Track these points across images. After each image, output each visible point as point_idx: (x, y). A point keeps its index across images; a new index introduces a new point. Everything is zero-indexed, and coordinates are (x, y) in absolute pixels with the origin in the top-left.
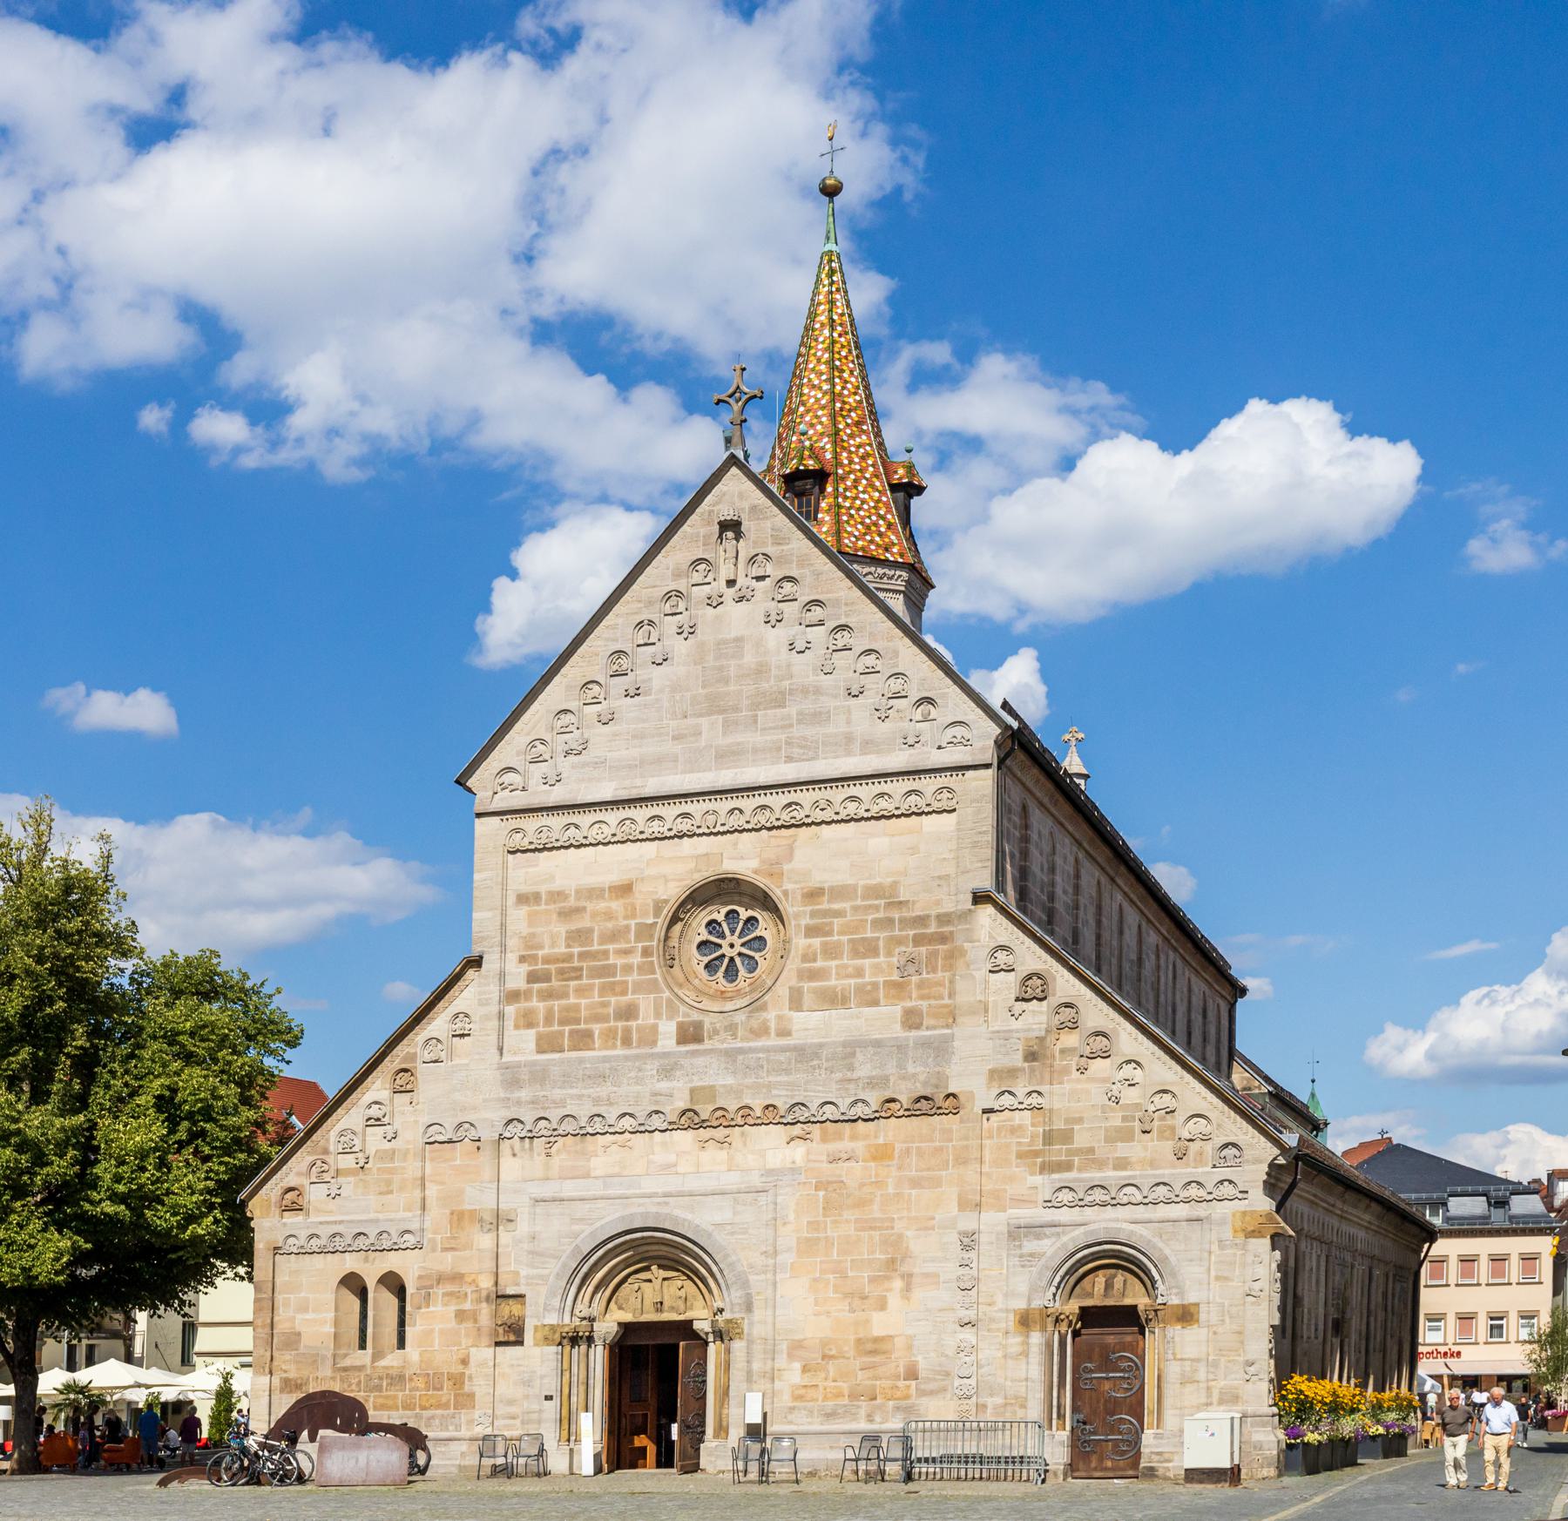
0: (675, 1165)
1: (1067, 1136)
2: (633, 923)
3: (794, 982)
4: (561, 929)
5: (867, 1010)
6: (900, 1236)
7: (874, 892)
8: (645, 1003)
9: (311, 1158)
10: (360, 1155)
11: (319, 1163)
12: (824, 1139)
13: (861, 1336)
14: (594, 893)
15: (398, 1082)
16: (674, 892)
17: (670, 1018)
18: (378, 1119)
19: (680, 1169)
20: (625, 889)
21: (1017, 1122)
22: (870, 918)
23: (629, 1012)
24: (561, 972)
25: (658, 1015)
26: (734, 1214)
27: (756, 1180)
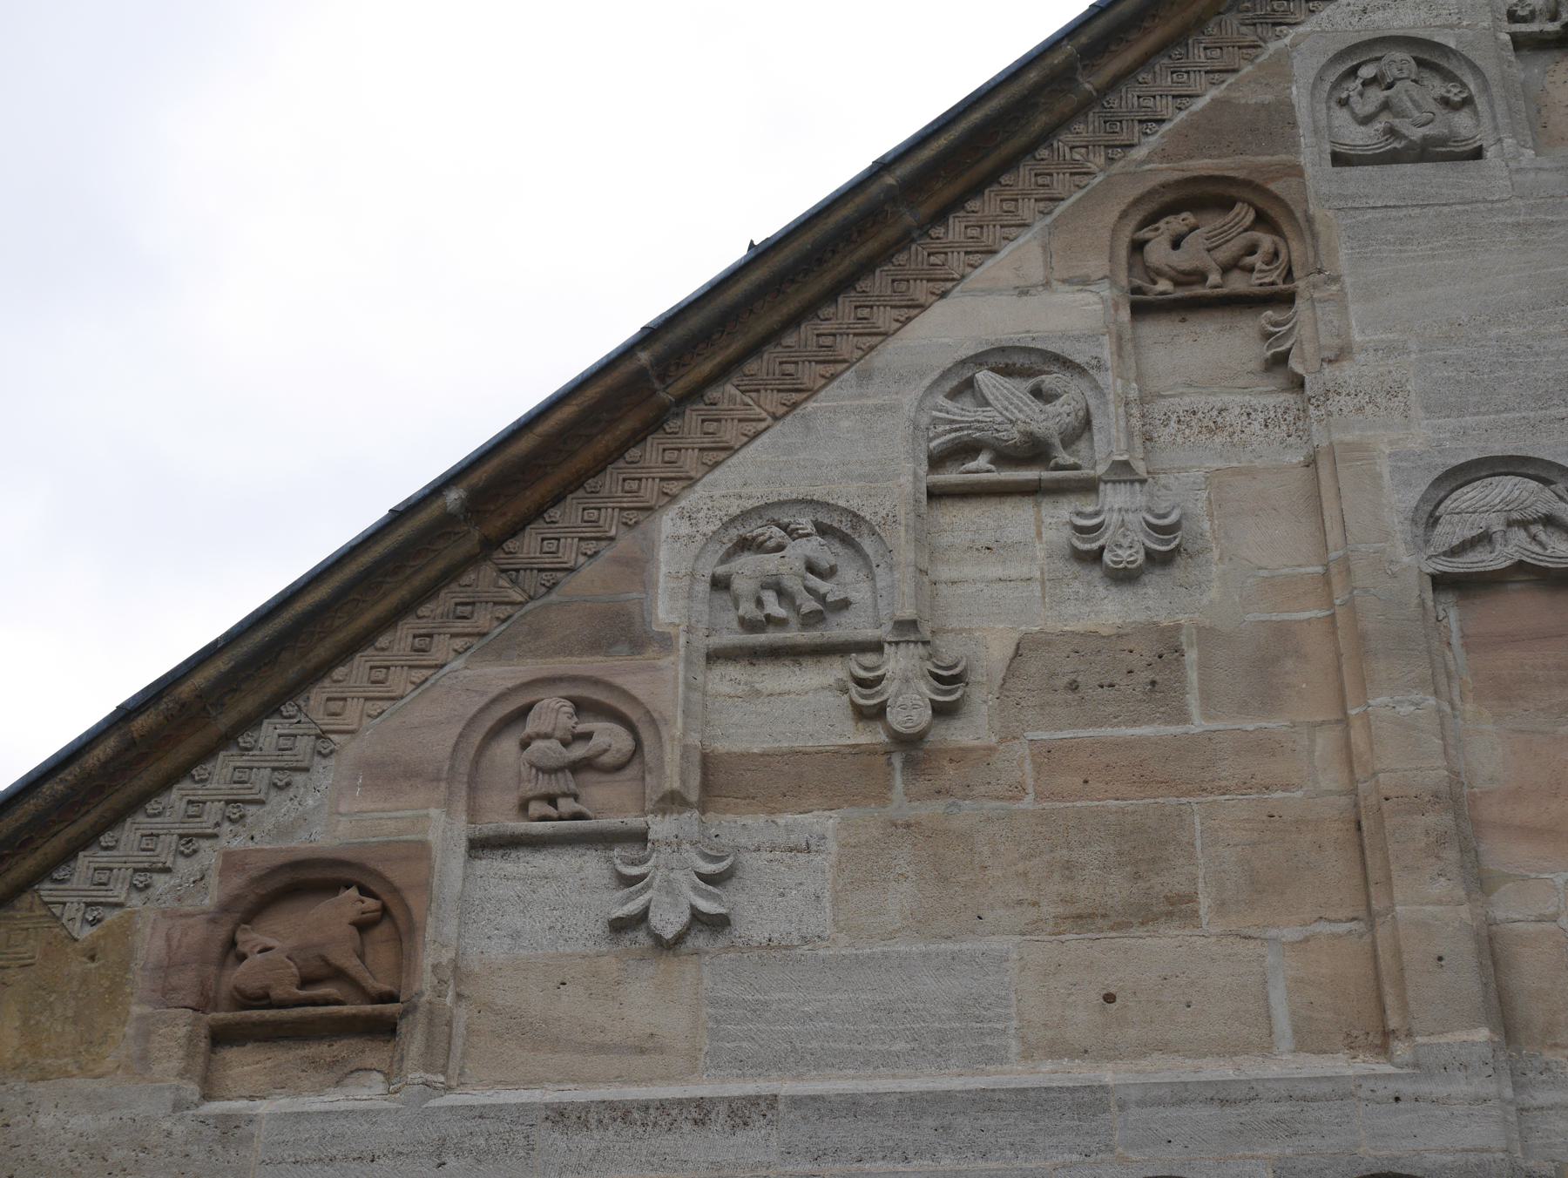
9: (500, 675)
10: (897, 663)
11: (553, 712)
15: (1158, 252)
18: (1035, 451)
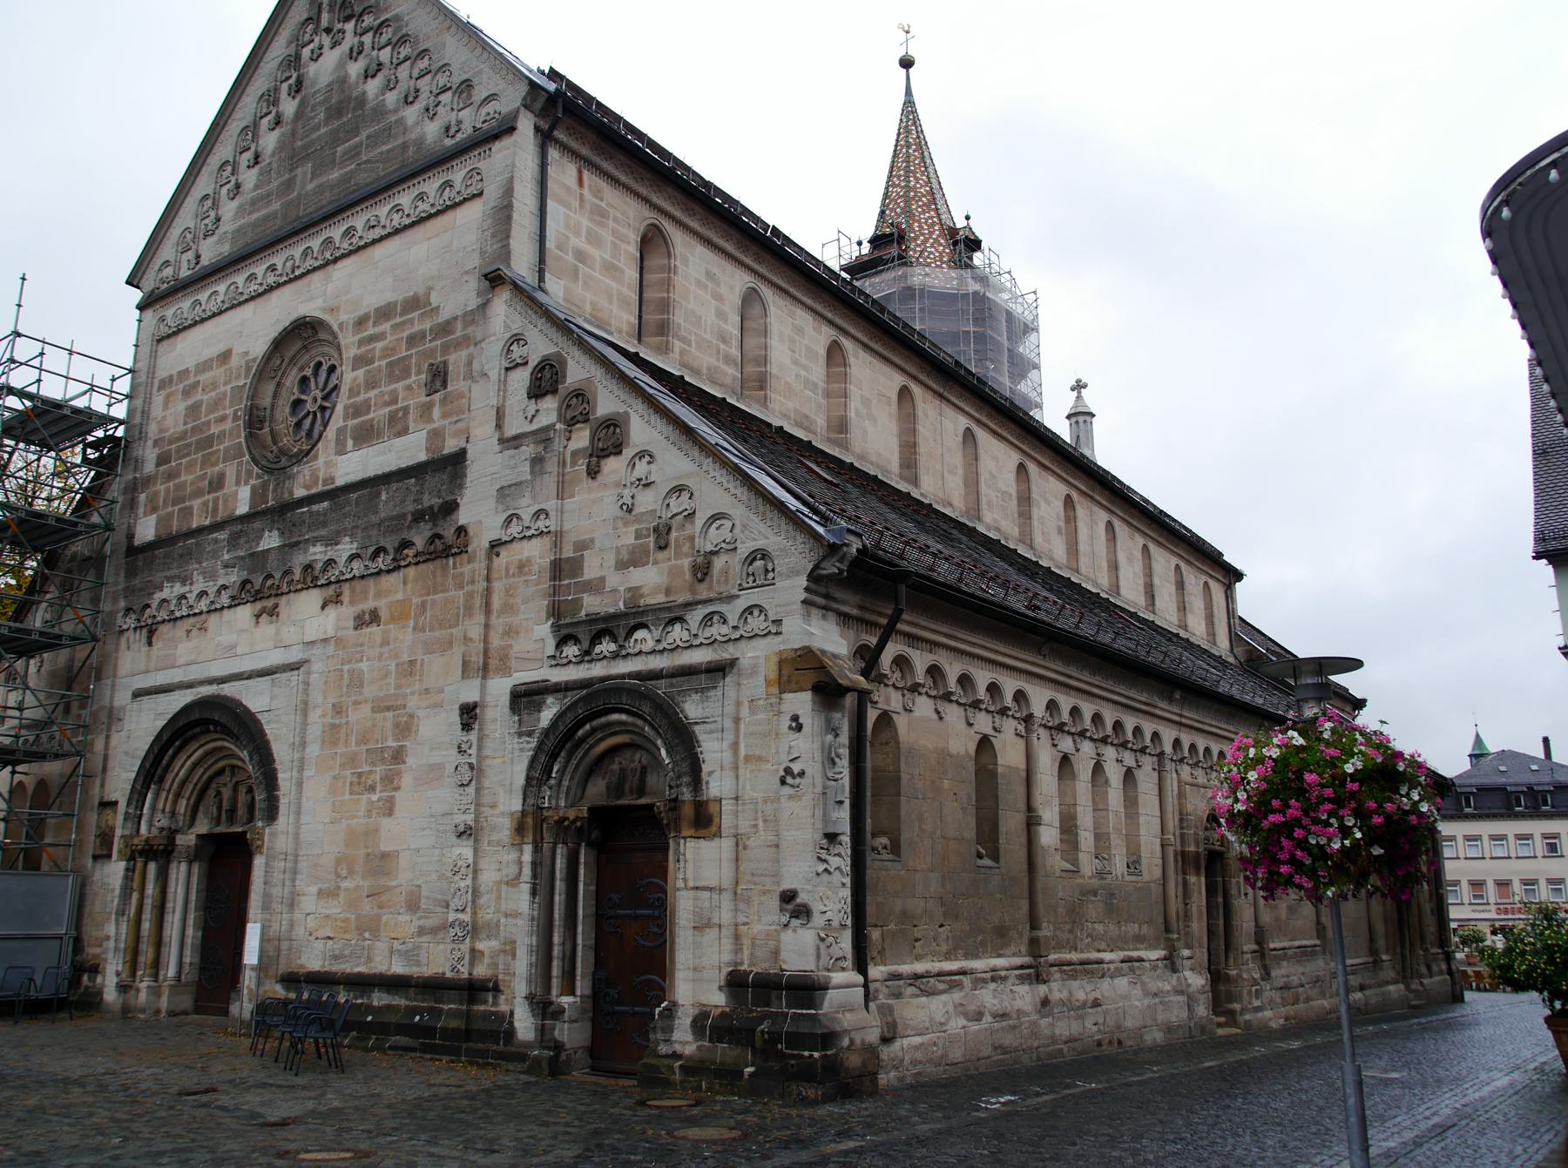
0: (234, 647)
1: (576, 566)
2: (228, 387)
3: (341, 423)
4: (181, 406)
5: (399, 442)
6: (411, 716)
7: (414, 303)
8: (231, 471)
12: (352, 603)
13: (370, 850)
14: (205, 366)
16: (259, 347)
17: (246, 483)
19: (239, 651)
20: (225, 356)
21: (526, 554)
22: (405, 335)
23: (217, 483)
24: (178, 450)
25: (238, 483)
26: (271, 699)
27: (294, 655)
